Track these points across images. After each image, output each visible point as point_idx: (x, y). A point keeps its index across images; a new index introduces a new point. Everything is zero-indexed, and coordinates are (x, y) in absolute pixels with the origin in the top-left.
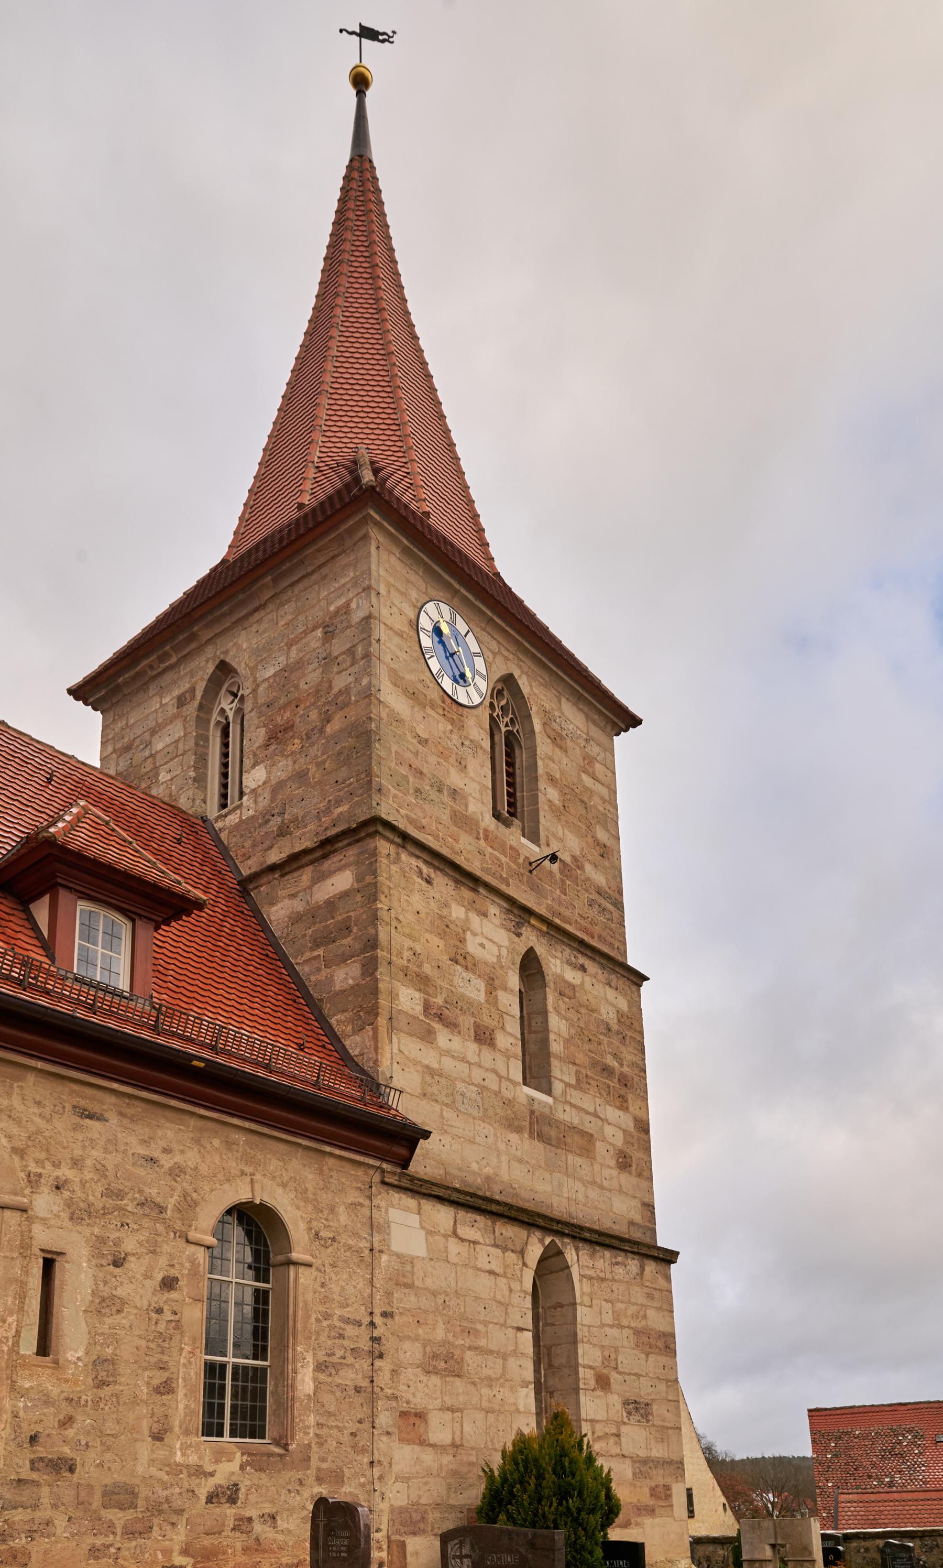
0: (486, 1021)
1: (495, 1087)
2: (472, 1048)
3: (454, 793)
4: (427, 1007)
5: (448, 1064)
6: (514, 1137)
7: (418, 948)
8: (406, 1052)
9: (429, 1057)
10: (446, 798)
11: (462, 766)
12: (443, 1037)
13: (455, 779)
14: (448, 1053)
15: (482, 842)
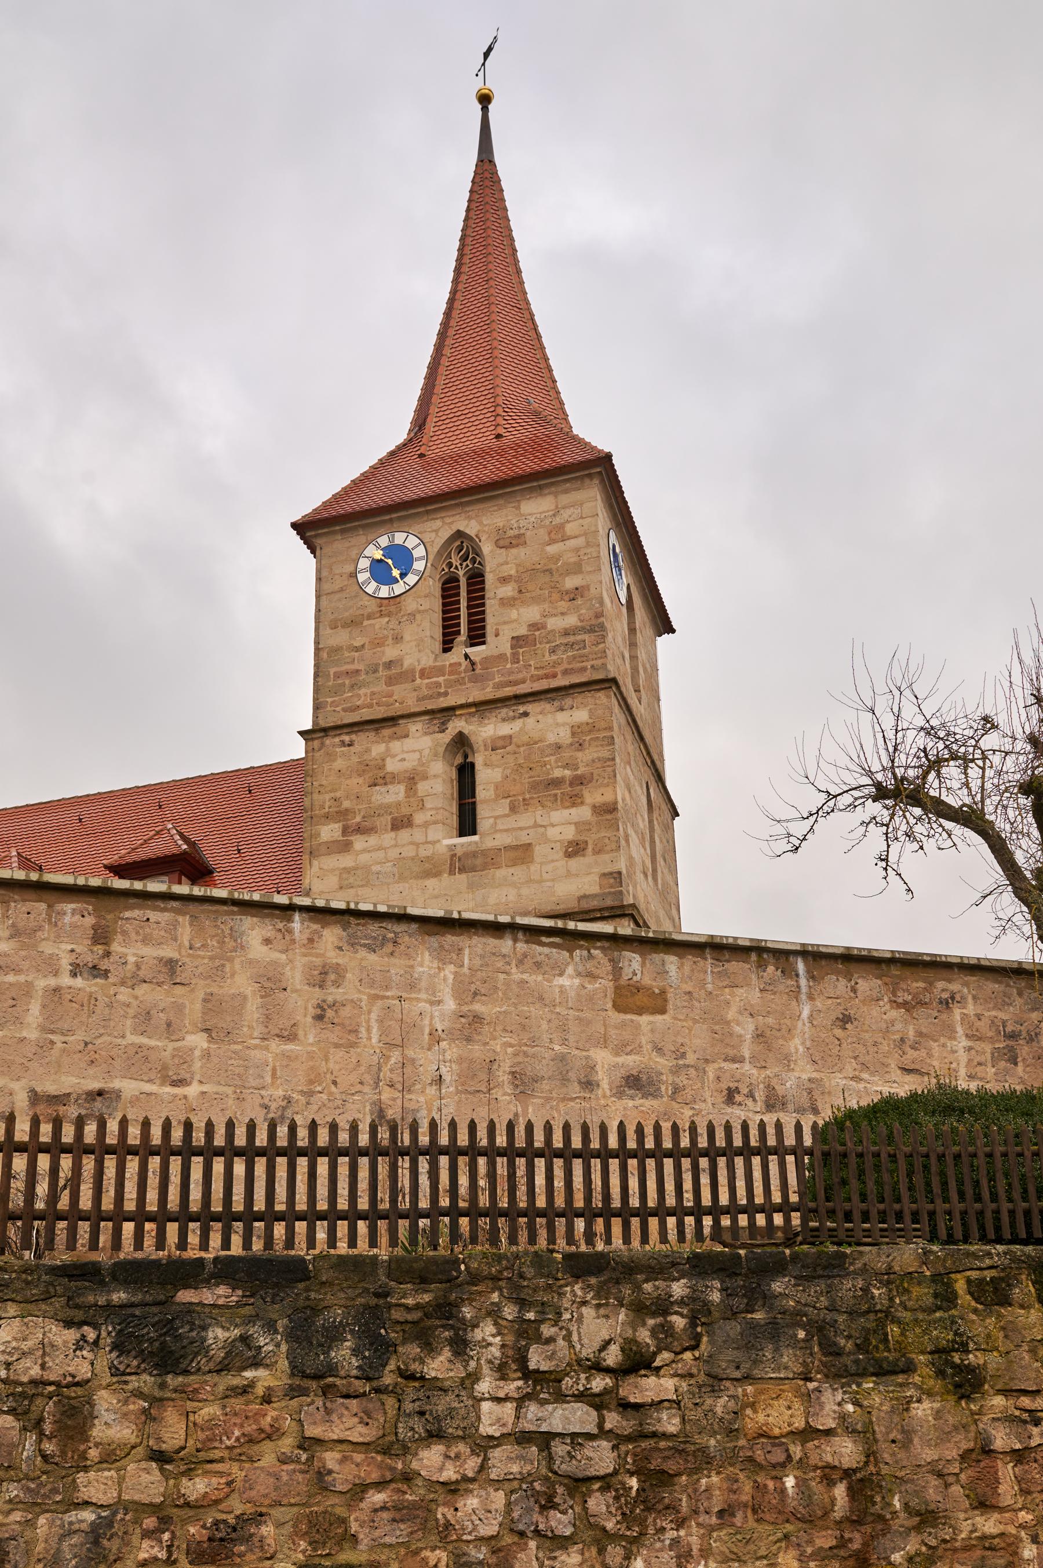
0: (405, 811)
1: (412, 854)
2: (388, 838)
3: (389, 665)
4: (345, 831)
5: (364, 858)
6: (431, 883)
7: (338, 794)
8: (325, 867)
9: (346, 861)
10: (382, 672)
11: (398, 639)
12: (359, 842)
13: (390, 652)
14: (365, 851)
15: (418, 681)
